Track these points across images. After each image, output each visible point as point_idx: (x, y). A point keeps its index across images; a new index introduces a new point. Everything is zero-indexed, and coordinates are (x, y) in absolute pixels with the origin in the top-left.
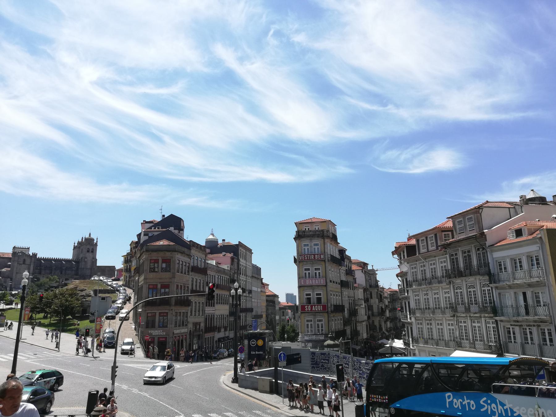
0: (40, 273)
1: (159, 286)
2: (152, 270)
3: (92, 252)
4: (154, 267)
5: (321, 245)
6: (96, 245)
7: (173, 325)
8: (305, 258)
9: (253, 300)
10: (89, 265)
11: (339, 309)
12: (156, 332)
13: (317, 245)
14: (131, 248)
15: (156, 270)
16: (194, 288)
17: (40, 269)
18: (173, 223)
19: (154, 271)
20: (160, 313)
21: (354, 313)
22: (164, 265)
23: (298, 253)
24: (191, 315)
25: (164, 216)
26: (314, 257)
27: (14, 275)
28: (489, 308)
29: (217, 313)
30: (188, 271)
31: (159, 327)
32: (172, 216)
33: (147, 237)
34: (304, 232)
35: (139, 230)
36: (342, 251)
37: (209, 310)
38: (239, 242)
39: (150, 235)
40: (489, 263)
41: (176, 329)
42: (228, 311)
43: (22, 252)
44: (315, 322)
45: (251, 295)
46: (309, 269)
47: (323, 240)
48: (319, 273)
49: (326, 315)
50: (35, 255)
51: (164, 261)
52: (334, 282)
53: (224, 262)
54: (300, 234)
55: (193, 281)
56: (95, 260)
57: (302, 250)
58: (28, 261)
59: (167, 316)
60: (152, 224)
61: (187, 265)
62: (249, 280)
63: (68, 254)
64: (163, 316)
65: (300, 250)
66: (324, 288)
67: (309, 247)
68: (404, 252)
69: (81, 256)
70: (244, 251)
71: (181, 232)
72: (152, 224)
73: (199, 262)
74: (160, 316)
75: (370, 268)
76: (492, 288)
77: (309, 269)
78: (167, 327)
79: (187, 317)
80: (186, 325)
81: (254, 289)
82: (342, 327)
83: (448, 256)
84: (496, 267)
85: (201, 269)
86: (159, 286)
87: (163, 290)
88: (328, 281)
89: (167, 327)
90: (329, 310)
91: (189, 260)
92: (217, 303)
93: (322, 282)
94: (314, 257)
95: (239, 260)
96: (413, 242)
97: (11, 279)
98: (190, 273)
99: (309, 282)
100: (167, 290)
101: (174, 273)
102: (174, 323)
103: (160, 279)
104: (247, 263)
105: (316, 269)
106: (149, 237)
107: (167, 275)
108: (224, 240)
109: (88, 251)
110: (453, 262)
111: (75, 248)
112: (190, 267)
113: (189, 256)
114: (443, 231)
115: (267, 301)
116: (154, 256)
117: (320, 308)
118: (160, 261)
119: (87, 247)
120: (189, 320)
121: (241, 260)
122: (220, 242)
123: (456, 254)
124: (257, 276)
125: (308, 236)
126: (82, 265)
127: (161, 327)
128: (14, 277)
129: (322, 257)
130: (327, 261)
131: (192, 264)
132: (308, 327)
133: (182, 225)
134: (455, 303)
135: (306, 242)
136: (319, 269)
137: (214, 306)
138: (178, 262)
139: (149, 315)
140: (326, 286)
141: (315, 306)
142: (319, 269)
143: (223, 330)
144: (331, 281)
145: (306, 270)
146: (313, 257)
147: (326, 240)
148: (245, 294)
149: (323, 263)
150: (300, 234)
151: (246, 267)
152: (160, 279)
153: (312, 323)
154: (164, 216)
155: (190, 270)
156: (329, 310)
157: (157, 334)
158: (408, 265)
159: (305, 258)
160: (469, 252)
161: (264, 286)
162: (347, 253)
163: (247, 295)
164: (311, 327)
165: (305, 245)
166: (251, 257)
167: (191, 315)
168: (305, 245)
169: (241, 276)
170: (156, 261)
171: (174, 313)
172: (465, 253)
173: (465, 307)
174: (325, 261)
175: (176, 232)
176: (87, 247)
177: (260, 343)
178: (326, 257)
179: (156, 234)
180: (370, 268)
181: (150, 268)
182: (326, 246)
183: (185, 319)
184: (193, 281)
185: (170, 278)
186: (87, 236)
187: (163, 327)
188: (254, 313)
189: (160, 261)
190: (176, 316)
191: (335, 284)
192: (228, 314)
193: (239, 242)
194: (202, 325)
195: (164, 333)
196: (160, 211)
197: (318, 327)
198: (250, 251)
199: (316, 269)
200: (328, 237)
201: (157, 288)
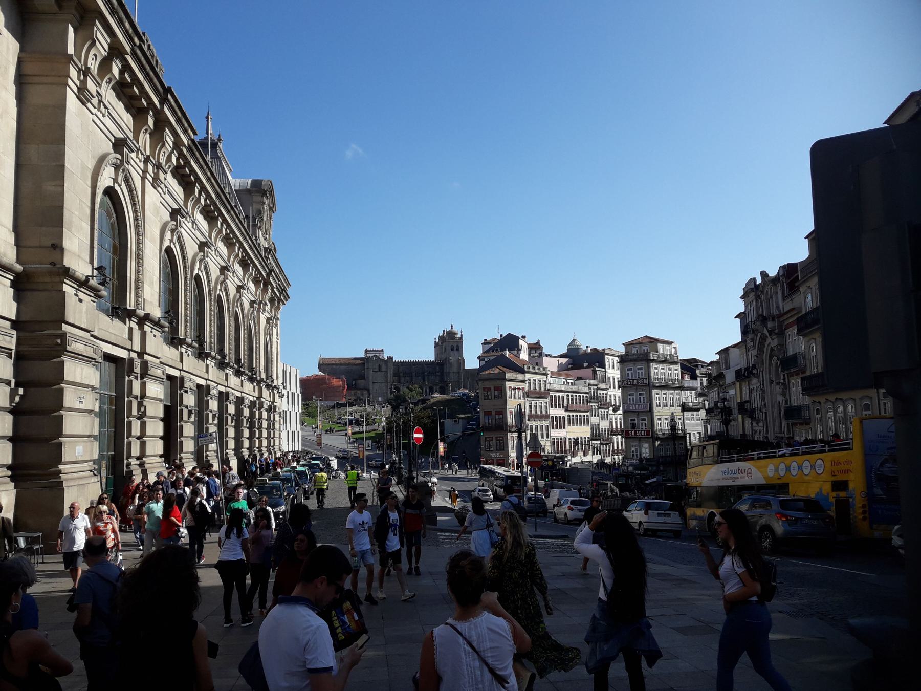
0: (399, 382)
1: (493, 413)
2: (486, 398)
3: (458, 350)
6: (461, 339)
10: (455, 369)
16: (533, 412)
17: (399, 377)
22: (496, 393)
27: (371, 384)
37: (556, 433)
43: (375, 356)
50: (390, 359)
55: (530, 407)
56: (461, 362)
58: (383, 368)
63: (428, 354)
69: (444, 356)
77: (632, 395)
85: (540, 392)
86: (493, 413)
87: (497, 417)
93: (646, 408)
97: (369, 391)
109: (452, 350)
111: (436, 345)
116: (487, 384)
117: (644, 433)
119: (450, 343)
125: (631, 361)
126: (446, 370)
128: (371, 389)
129: (645, 381)
135: (629, 366)
137: (564, 428)
165: (629, 370)
168: (629, 370)
170: (489, 389)
174: (649, 385)
176: (450, 343)
179: (492, 358)
184: (530, 407)
186: (449, 329)
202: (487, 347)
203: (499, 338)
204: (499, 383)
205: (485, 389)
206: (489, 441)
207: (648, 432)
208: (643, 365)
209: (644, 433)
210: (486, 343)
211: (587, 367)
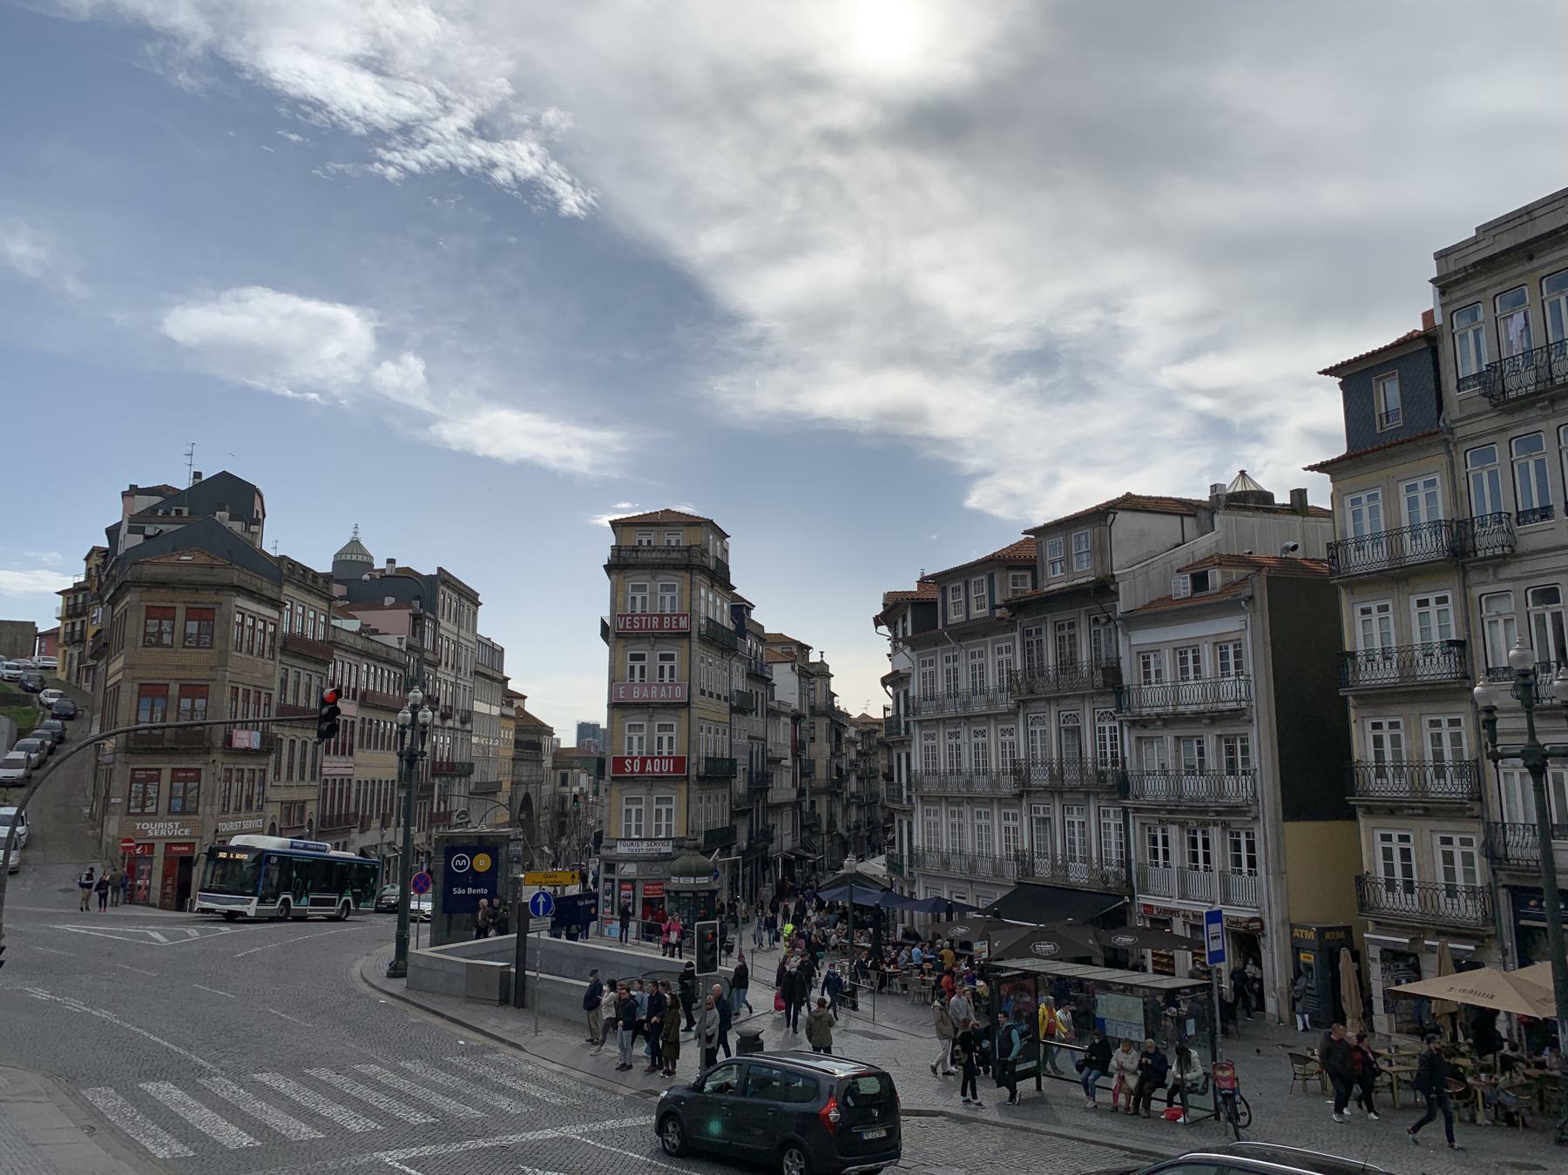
1: (174, 689)
2: (153, 641)
4: (161, 633)
5: (681, 590)
7: (217, 808)
8: (632, 624)
9: (475, 740)
11: (718, 773)
12: (162, 829)
13: (671, 588)
14: (89, 570)
15: (166, 639)
18: (232, 497)
19: (159, 644)
20: (174, 770)
21: (760, 784)
22: (193, 627)
23: (613, 611)
24: (277, 772)
25: (197, 475)
26: (661, 623)
28: (1109, 777)
29: (361, 774)
30: (272, 649)
31: (170, 812)
32: (225, 478)
33: (139, 539)
34: (635, 549)
35: (115, 515)
36: (741, 609)
37: (333, 765)
38: (440, 569)
39: (150, 531)
40: (1118, 659)
41: (227, 821)
42: (396, 771)
44: (649, 804)
45: (468, 727)
46: (642, 657)
47: (687, 576)
48: (672, 668)
49: (683, 787)
51: (191, 614)
52: (711, 695)
53: (393, 627)
54: (623, 554)
55: (284, 682)
57: (625, 601)
59: (198, 780)
60: (157, 499)
61: (271, 628)
62: (467, 682)
64: (185, 780)
65: (620, 600)
66: (684, 714)
67: (647, 594)
68: (904, 620)
70: (455, 596)
71: (253, 528)
72: (157, 499)
73: (310, 625)
74: (174, 779)
75: (814, 657)
76: (1121, 723)
77: (642, 657)
78: (196, 812)
79: (263, 783)
80: (260, 808)
81: (480, 707)
82: (727, 818)
83: (1017, 634)
84: (1135, 668)
86: (174, 689)
87: (186, 703)
88: (695, 691)
89: (196, 812)
90: (693, 772)
91: (276, 615)
92: (361, 746)
93: (679, 695)
94: (661, 623)
95: (436, 622)
96: (933, 593)
98: (278, 657)
99: (637, 695)
100: (200, 703)
101: (224, 653)
102: (218, 801)
103: (178, 667)
104: (463, 633)
105: (663, 657)
106: (147, 537)
107: (204, 656)
108: (391, 561)
110: (1030, 652)
112: (279, 635)
113: (277, 605)
114: (1010, 568)
115: (517, 743)
116: (160, 598)
117: (668, 767)
118: (180, 614)
120: (269, 792)
121: (443, 623)
122: (380, 564)
123: (1039, 631)
124: (489, 672)
127: (175, 813)
129: (683, 623)
130: (694, 635)
131: (286, 629)
132: (628, 819)
133: (257, 507)
134: (1027, 759)
136: (671, 657)
137: (351, 754)
138: (238, 618)
139: (141, 775)
140: (688, 705)
141: (653, 759)
142: (671, 657)
143: (376, 823)
144: (703, 692)
145: (634, 657)
146: (655, 623)
147: (698, 578)
148: (450, 723)
149: (685, 643)
150: (623, 554)
151: (457, 644)
152: (178, 667)
153: (642, 807)
154: (197, 475)
155: (279, 644)
156: (693, 772)
157: (163, 833)
158: (913, 656)
159: (632, 624)
160: (1071, 625)
161: (513, 698)
162: (755, 615)
163: (458, 725)
164: (639, 819)
166: (475, 614)
167: (277, 772)
169: (442, 668)
171: (221, 773)
172: (1061, 627)
173: (1051, 770)
174: (688, 635)
175: (237, 527)
177: (482, 863)
178: (695, 623)
180: (814, 657)
181: (146, 634)
182: (695, 594)
183: (257, 789)
185: (212, 668)
187: (184, 812)
188: (475, 778)
189: (180, 614)
190: (229, 780)
191: (714, 700)
192: (395, 778)
193: (440, 569)
194: (312, 809)
195: (187, 832)
196: (188, 460)
197: (658, 817)
198: (472, 598)
199: (663, 657)
200: (703, 569)
201: (166, 696)
202: (143, 503)
203: (183, 483)
204: (207, 598)
205: (151, 612)
206: (145, 781)
207: (679, 763)
208: (679, 580)
209: (668, 767)
210: (134, 491)
211: (392, 607)
